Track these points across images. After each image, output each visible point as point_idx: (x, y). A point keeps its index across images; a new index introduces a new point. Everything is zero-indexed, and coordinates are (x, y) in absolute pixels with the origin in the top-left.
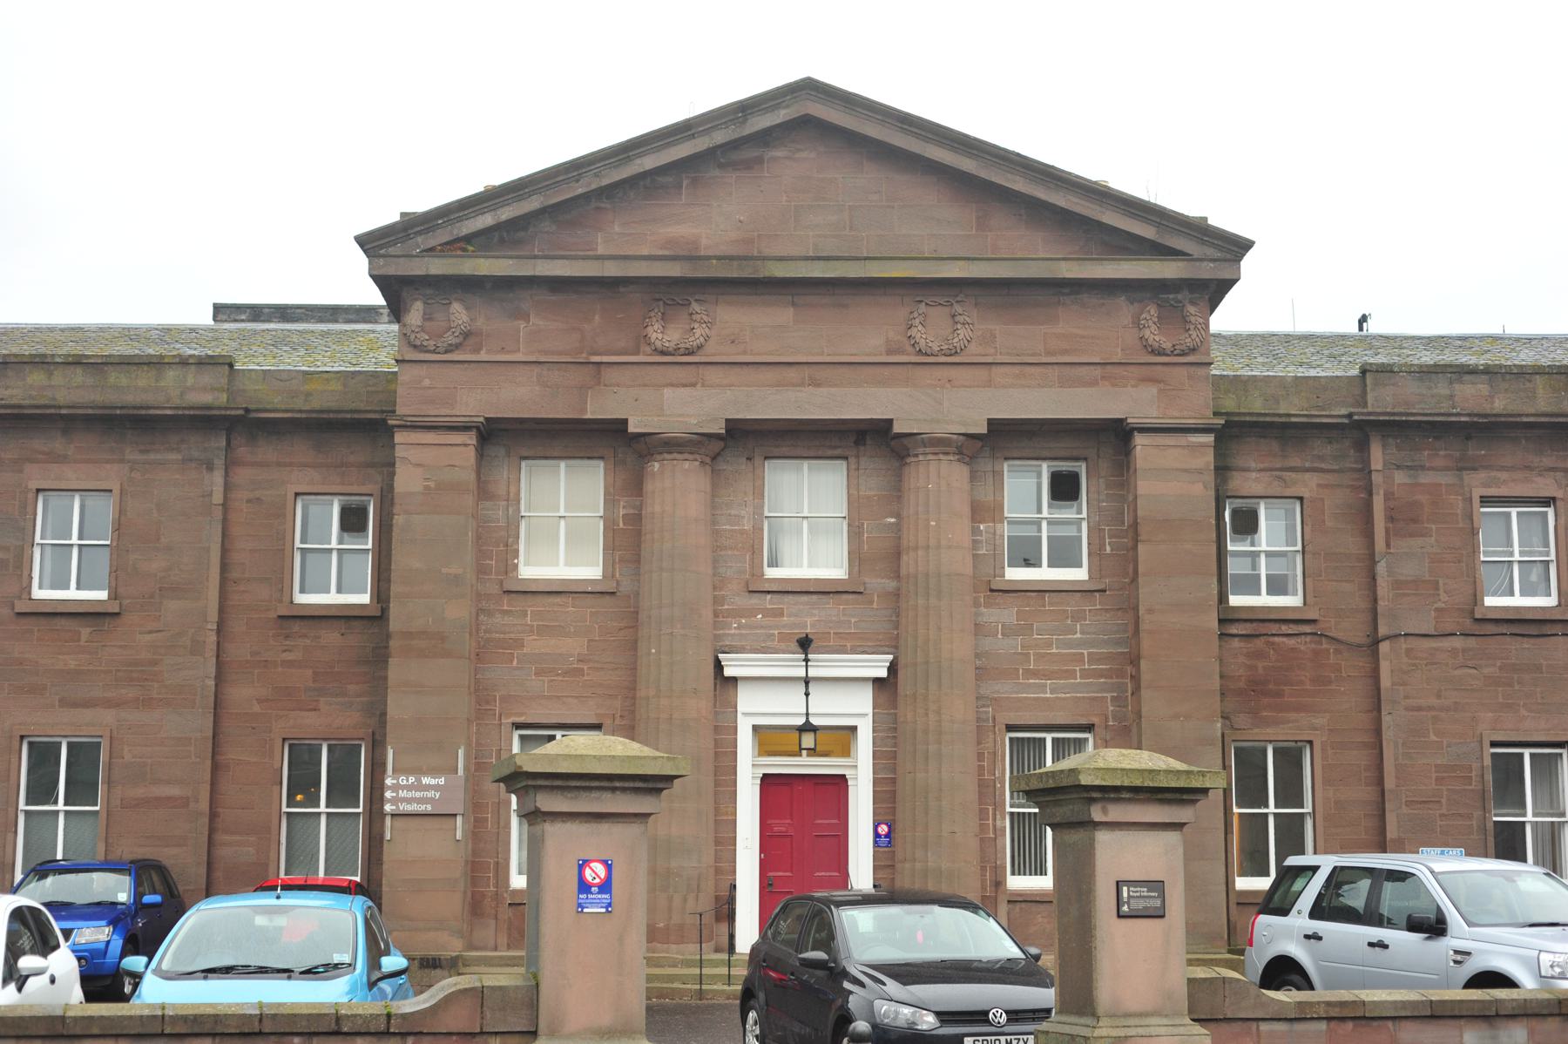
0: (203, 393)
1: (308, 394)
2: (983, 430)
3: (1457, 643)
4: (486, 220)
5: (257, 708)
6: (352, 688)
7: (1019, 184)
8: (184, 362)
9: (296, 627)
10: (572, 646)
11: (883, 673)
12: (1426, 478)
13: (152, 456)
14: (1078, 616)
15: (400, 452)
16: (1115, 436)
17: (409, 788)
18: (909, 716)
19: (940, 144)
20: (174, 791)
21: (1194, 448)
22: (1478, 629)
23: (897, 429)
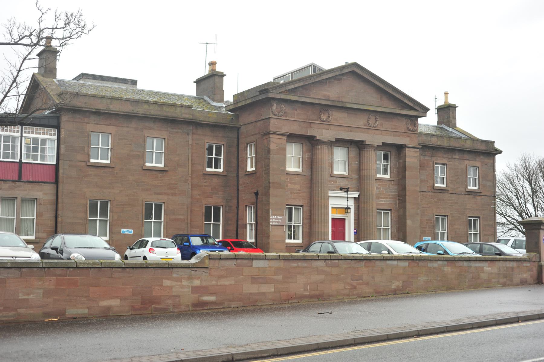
0: (185, 115)
1: (209, 117)
2: (381, 145)
3: (430, 194)
4: (292, 87)
5: (198, 197)
6: (220, 193)
7: (390, 91)
8: (182, 106)
9: (207, 177)
10: (297, 187)
11: (357, 196)
12: (426, 158)
13: (175, 130)
14: (389, 186)
15: (271, 140)
16: (400, 148)
17: (275, 219)
18: (365, 206)
19: (377, 80)
20: (182, 217)
21: (415, 151)
22: (433, 191)
23: (367, 143)
